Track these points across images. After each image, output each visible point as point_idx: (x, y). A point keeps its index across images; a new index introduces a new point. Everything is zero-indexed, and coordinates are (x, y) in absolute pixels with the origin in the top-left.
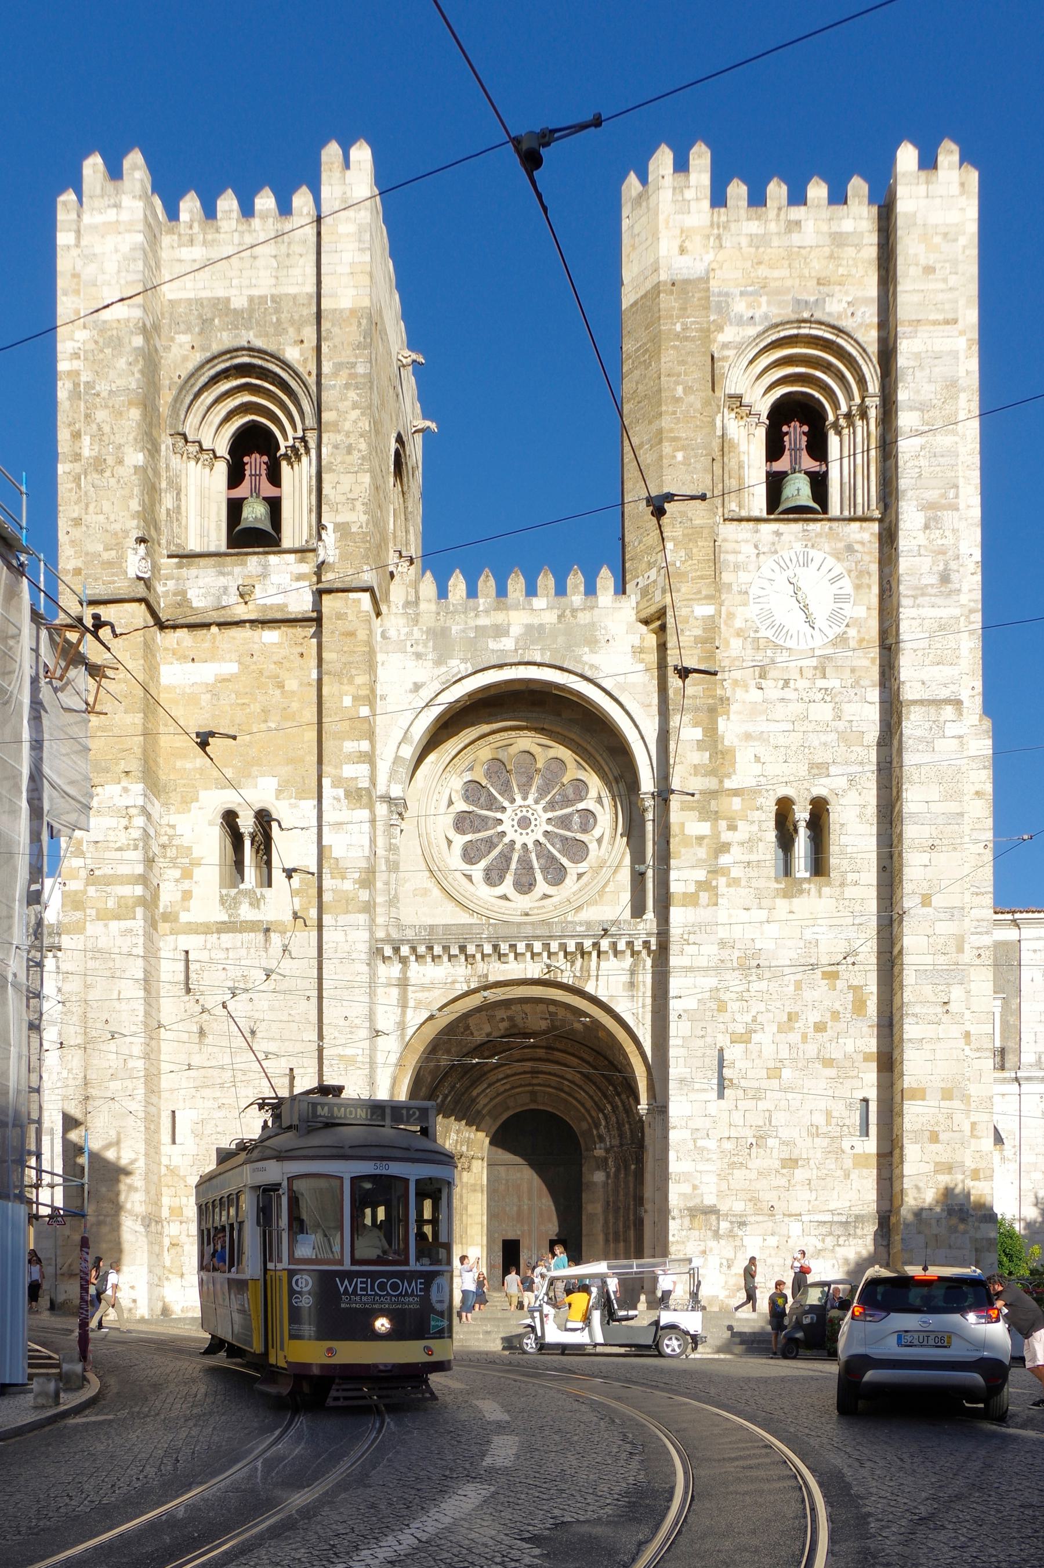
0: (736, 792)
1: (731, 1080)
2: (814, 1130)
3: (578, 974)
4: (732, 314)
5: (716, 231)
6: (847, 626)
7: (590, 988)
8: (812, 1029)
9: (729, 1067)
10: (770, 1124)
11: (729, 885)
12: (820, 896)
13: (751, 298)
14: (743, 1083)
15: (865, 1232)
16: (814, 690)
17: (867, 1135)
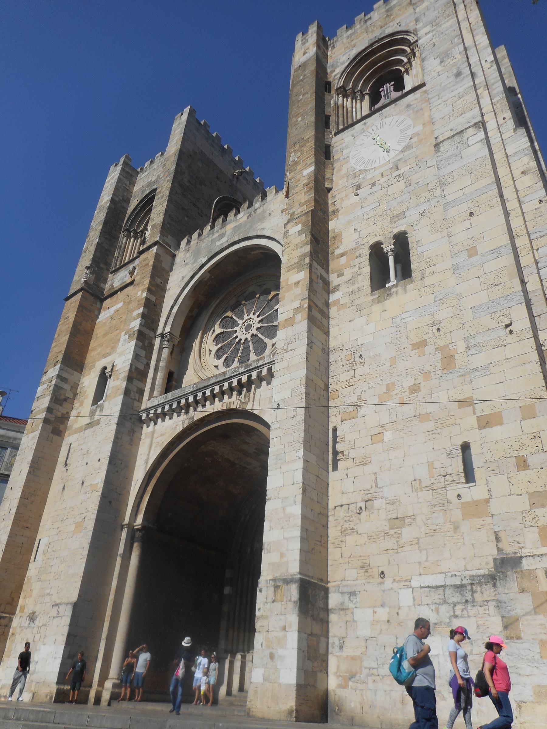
0: (342, 255)
1: (342, 452)
2: (417, 484)
3: (243, 401)
4: (339, 64)
5: (332, 45)
6: (411, 139)
7: (248, 408)
8: (407, 393)
9: (341, 442)
10: (376, 486)
11: (339, 310)
12: (406, 291)
13: (348, 53)
14: (353, 454)
15: (486, 597)
16: (391, 180)
17: (474, 481)
